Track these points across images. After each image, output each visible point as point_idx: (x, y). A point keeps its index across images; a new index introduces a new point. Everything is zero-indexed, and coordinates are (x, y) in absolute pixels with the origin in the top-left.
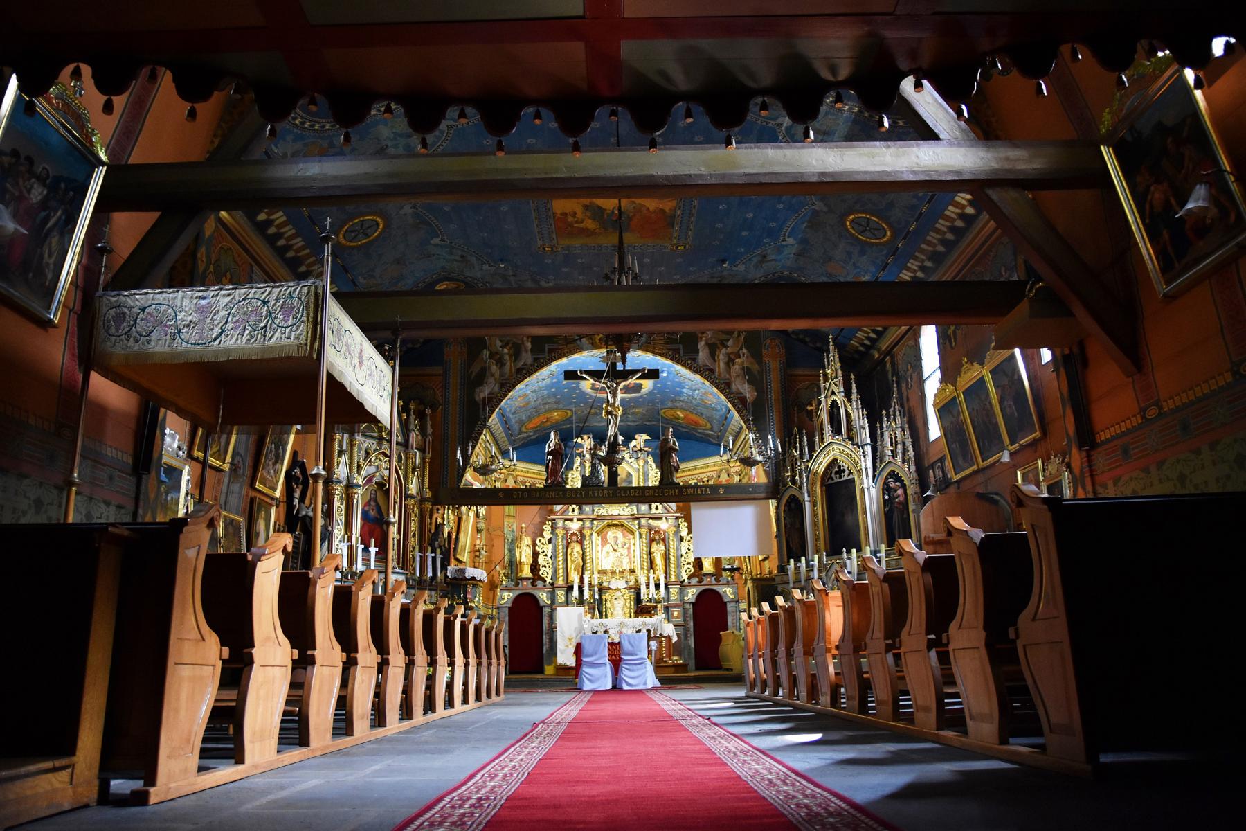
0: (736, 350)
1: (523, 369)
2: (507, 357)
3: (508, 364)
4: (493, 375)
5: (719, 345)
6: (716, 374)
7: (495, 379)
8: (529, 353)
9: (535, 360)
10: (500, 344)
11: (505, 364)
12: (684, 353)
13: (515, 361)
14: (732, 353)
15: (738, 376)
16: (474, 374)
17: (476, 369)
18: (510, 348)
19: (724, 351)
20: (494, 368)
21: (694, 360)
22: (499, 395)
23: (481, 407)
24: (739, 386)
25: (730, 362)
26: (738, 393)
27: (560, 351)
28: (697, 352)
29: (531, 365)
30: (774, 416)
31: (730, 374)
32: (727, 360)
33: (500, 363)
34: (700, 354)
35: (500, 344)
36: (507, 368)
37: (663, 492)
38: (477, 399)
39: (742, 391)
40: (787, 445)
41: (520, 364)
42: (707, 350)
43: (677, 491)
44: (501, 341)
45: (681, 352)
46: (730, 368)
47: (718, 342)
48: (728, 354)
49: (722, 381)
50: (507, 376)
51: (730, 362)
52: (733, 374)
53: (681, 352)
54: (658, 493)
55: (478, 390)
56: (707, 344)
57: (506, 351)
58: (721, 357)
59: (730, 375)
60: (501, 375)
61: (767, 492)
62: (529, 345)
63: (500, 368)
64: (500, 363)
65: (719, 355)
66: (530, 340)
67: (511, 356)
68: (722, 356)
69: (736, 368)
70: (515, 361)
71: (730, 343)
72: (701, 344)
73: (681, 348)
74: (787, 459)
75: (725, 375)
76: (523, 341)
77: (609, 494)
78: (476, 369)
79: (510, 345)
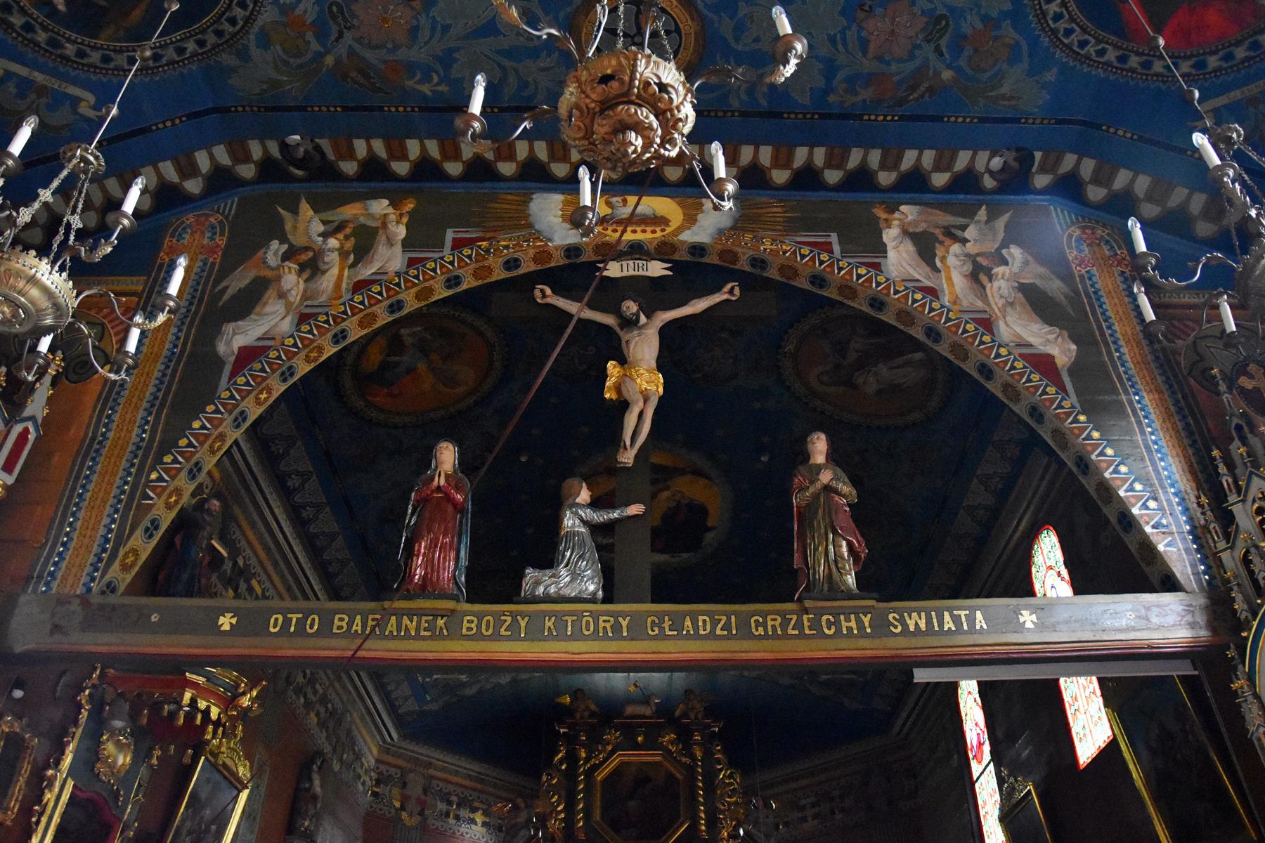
0: (991, 246)
1: (373, 282)
2: (335, 256)
3: (335, 271)
4: (282, 295)
5: (941, 237)
6: (946, 300)
7: (288, 306)
8: (398, 248)
9: (411, 263)
10: (321, 228)
11: (324, 272)
12: (844, 252)
13: (353, 266)
14: (978, 255)
15: (1011, 304)
16: (230, 293)
17: (238, 281)
18: (347, 238)
19: (956, 248)
20: (292, 280)
21: (877, 267)
22: (291, 341)
23: (228, 369)
24: (1018, 330)
25: (978, 273)
26: (1019, 345)
27: (485, 244)
28: (881, 249)
29: (398, 274)
30: (1146, 401)
31: (984, 297)
32: (968, 267)
33: (312, 267)
34: (891, 254)
35: (321, 228)
36: (327, 282)
37: (816, 625)
38: (221, 348)
39: (1032, 340)
40: (1222, 469)
41: (366, 272)
42: (908, 247)
43: (866, 620)
44: (324, 223)
45: (836, 248)
46: (984, 287)
47: (937, 232)
48: (972, 258)
49: (966, 317)
50: (322, 299)
51: (978, 273)
52: (996, 303)
53: (836, 248)
54: (799, 625)
55: (229, 328)
56: (905, 232)
57: (333, 243)
58: (951, 260)
59: (989, 305)
60: (305, 297)
61: (1192, 625)
62: (401, 232)
63: (306, 281)
64: (312, 267)
65: (943, 259)
66: (405, 220)
67: (343, 254)
68: (953, 259)
69: (1001, 286)
70: (353, 266)
71: (970, 233)
72: (890, 236)
73: (834, 238)
74: (1237, 510)
75: (969, 300)
76: (384, 225)
77: (617, 628)
78: (238, 281)
79: (348, 231)
